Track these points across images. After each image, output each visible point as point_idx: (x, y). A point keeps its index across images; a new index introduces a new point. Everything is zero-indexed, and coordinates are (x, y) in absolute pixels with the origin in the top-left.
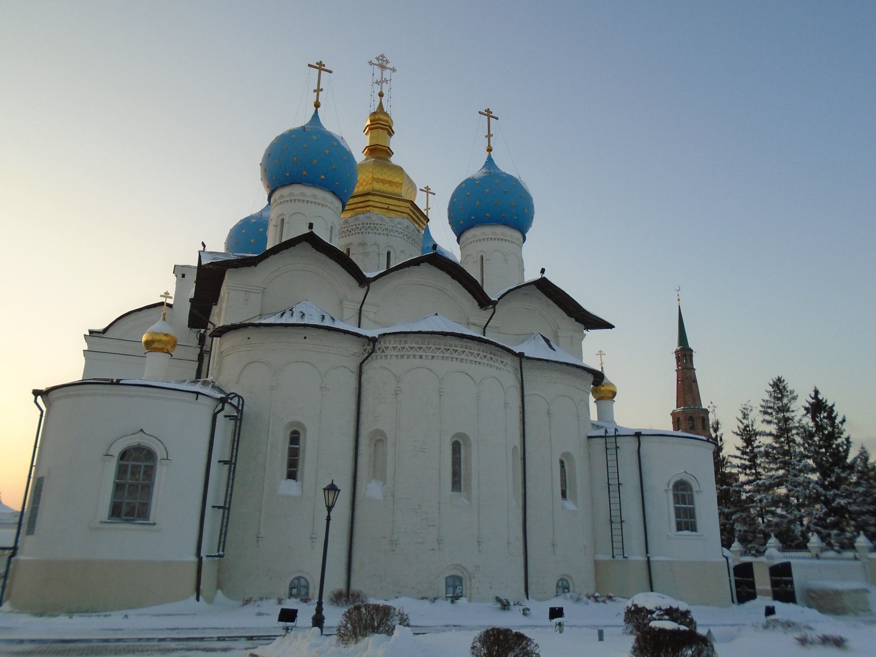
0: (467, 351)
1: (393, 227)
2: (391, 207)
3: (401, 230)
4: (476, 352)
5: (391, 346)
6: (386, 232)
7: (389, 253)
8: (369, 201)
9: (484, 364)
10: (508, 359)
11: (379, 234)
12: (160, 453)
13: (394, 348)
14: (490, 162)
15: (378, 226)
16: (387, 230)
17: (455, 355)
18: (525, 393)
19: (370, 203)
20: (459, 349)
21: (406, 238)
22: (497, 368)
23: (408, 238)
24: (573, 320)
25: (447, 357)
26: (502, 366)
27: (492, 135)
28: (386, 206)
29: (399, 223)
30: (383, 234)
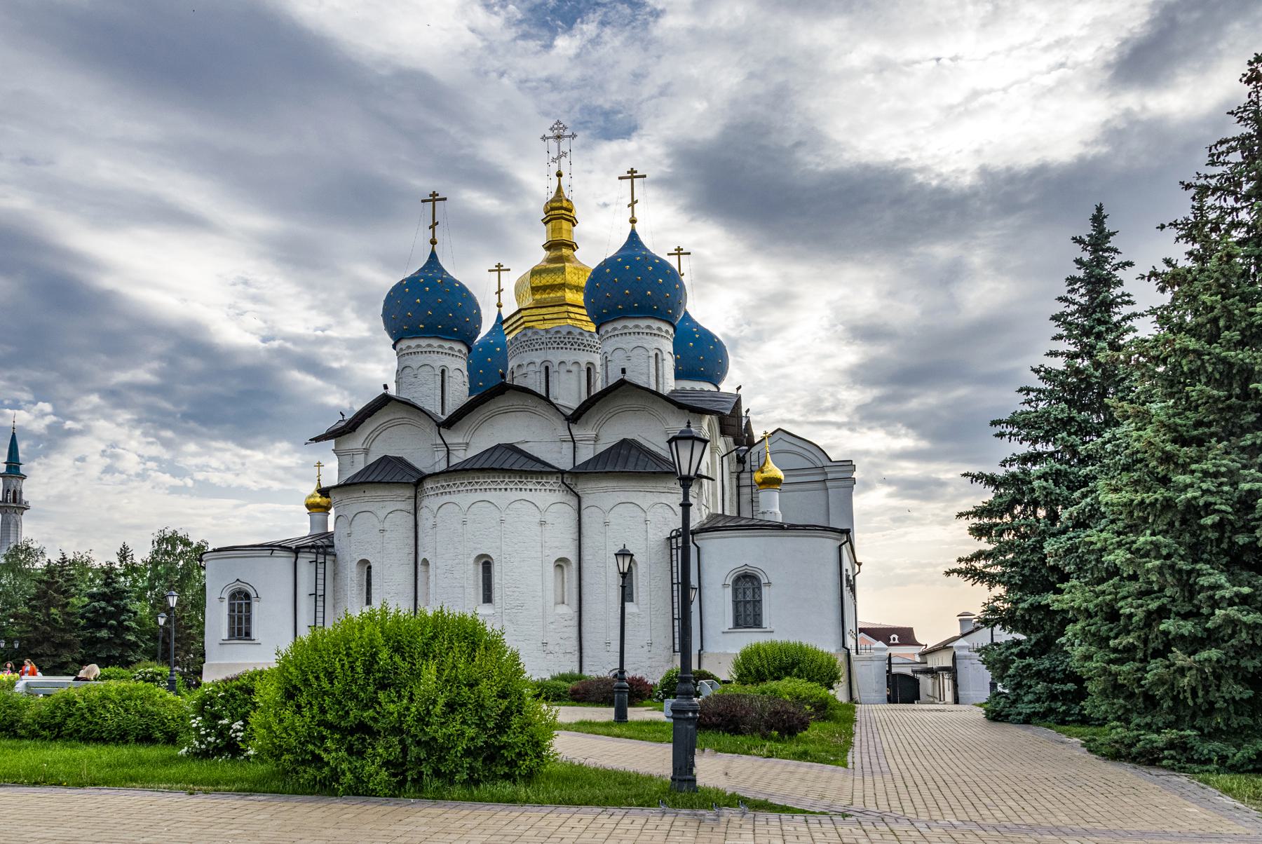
0: (489, 481)
1: (550, 338)
2: (546, 317)
3: (562, 339)
4: (499, 480)
5: (429, 487)
6: (542, 347)
7: (547, 368)
8: (522, 317)
9: (511, 489)
10: (552, 480)
11: (537, 350)
12: (253, 595)
13: (432, 488)
14: (633, 235)
15: (534, 342)
16: (543, 343)
17: (477, 487)
18: (583, 506)
19: (525, 319)
20: (482, 480)
21: (569, 346)
22: (531, 490)
23: (572, 345)
24: (687, 411)
25: (471, 490)
26: (539, 487)
27: (637, 202)
28: (541, 317)
29: (558, 332)
30: (541, 349)
